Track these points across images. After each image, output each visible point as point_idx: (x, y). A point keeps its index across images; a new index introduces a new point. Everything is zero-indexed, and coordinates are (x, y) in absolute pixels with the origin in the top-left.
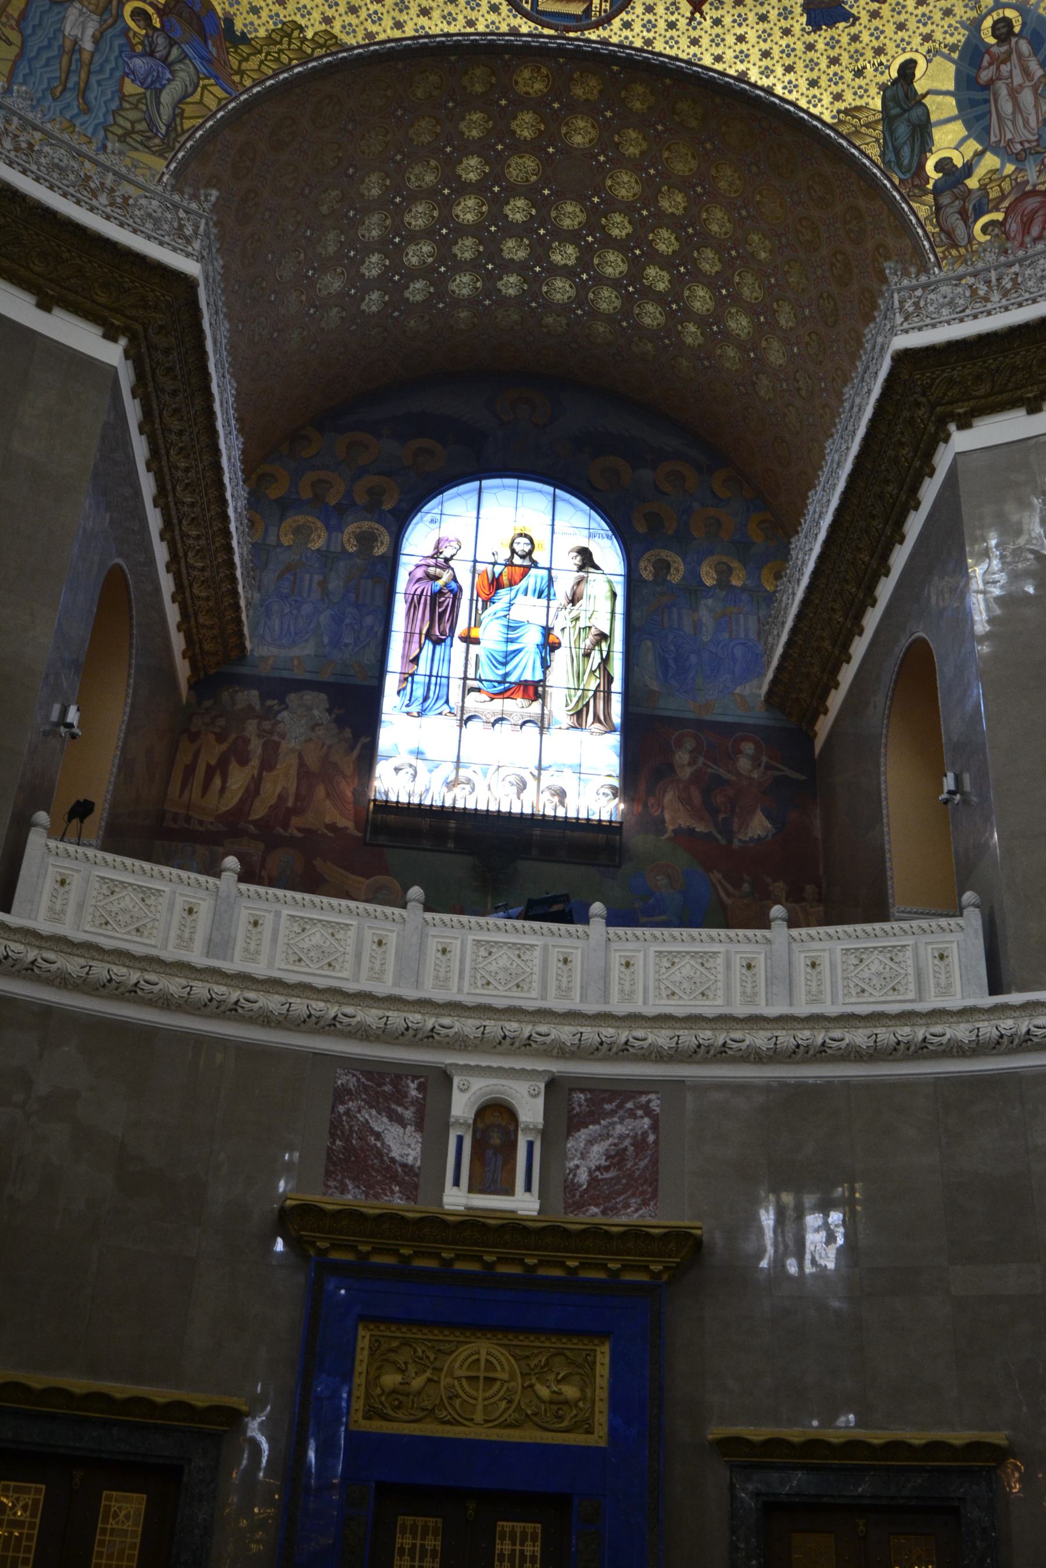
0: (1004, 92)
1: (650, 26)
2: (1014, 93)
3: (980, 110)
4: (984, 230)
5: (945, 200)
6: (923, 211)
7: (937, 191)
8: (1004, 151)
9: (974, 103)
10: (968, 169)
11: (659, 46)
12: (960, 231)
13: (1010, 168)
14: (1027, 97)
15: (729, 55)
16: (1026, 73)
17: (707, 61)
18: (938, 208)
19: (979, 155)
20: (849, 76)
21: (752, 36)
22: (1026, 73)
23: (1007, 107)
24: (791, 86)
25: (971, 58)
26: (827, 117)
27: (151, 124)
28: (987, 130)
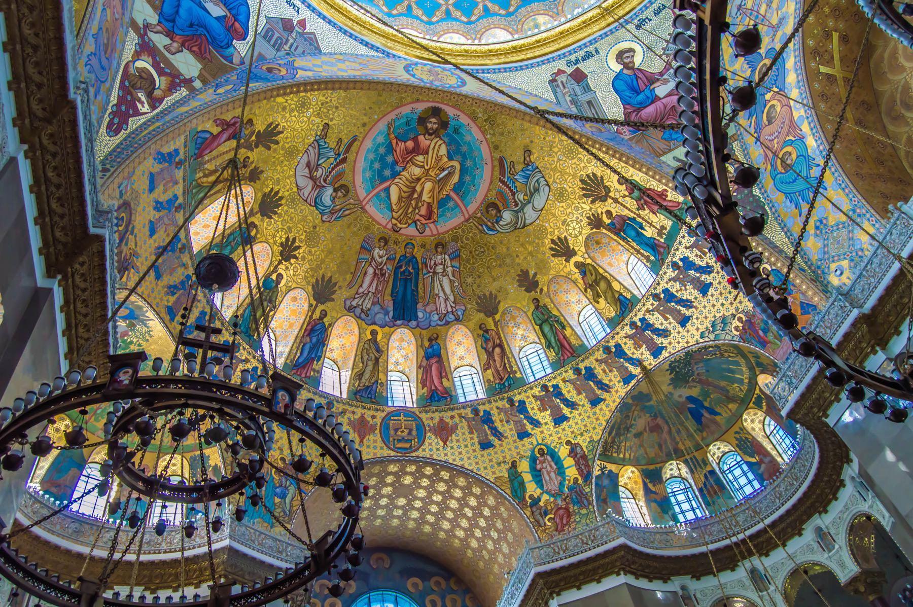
0: (545, 473)
1: (431, 450)
2: (548, 473)
3: (539, 479)
4: (549, 520)
5: (534, 509)
6: (528, 513)
7: (531, 506)
8: (549, 493)
9: (537, 476)
10: (539, 499)
11: (435, 457)
12: (541, 521)
13: (552, 499)
14: (553, 475)
15: (457, 459)
16: (551, 466)
17: (451, 461)
18: (533, 513)
19: (542, 494)
20: (496, 466)
21: (464, 452)
22: (551, 466)
23: (547, 477)
24: (479, 469)
25: (533, 460)
26: (492, 480)
27: (284, 512)
28: (542, 485)
